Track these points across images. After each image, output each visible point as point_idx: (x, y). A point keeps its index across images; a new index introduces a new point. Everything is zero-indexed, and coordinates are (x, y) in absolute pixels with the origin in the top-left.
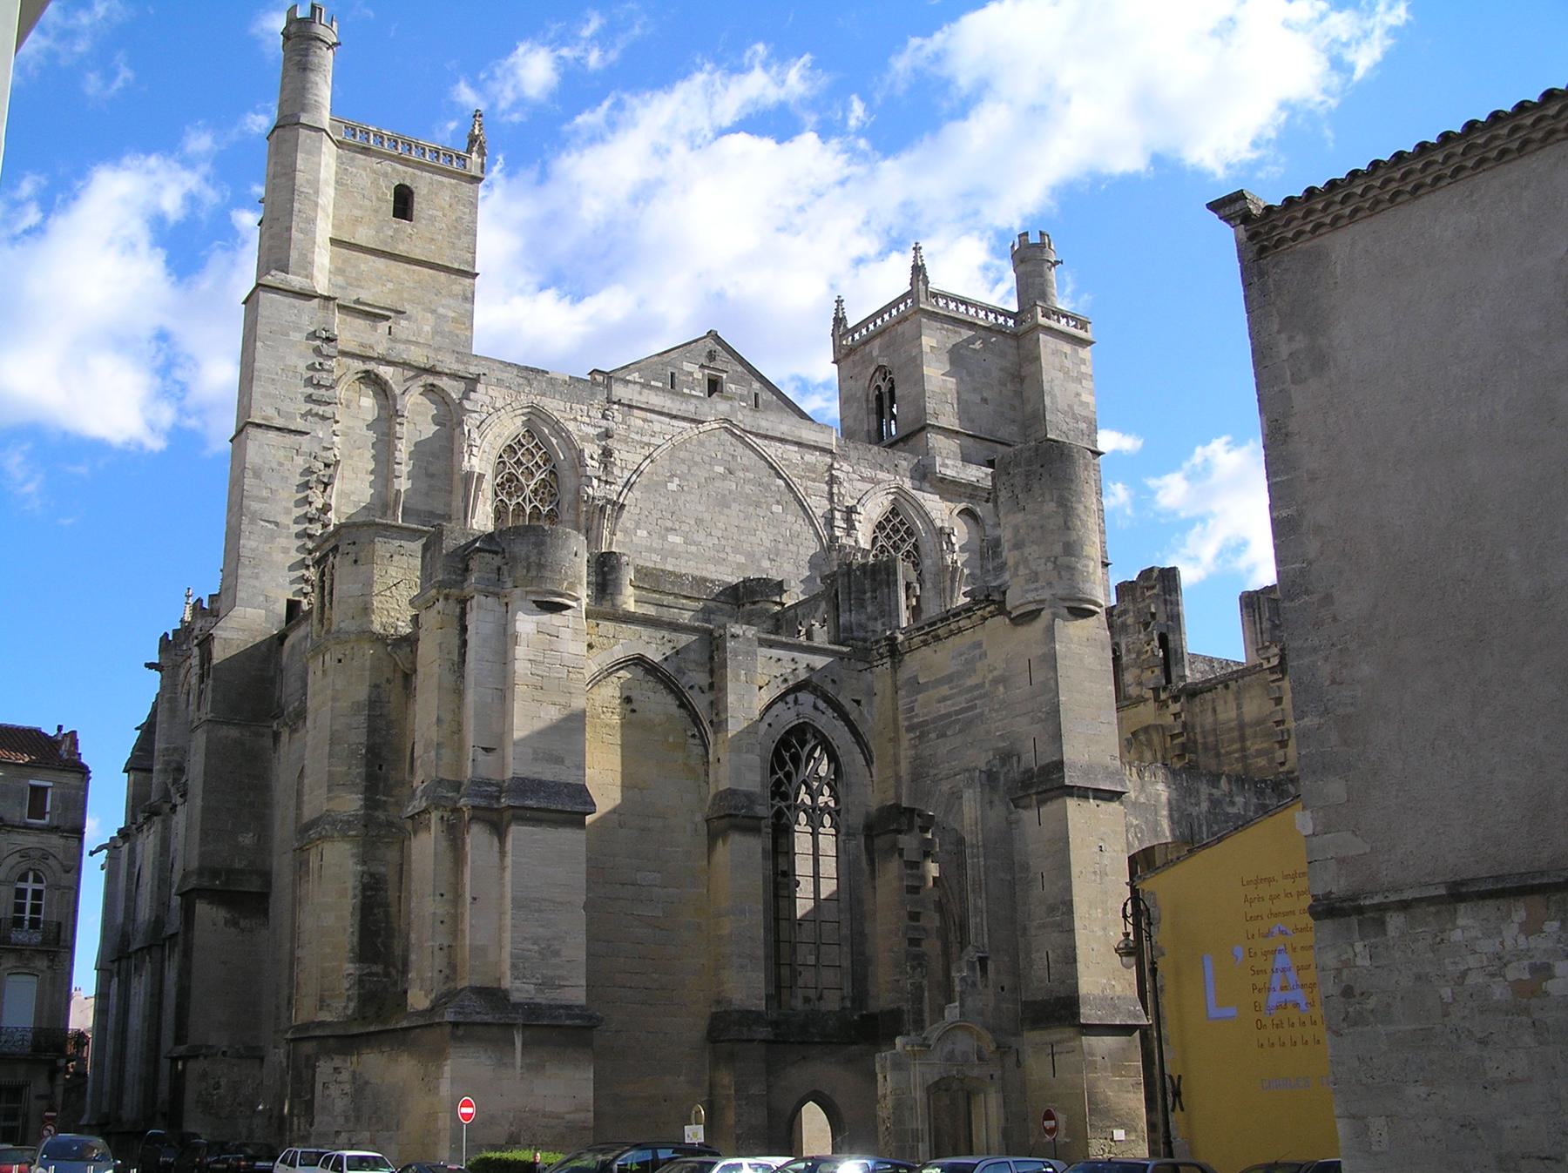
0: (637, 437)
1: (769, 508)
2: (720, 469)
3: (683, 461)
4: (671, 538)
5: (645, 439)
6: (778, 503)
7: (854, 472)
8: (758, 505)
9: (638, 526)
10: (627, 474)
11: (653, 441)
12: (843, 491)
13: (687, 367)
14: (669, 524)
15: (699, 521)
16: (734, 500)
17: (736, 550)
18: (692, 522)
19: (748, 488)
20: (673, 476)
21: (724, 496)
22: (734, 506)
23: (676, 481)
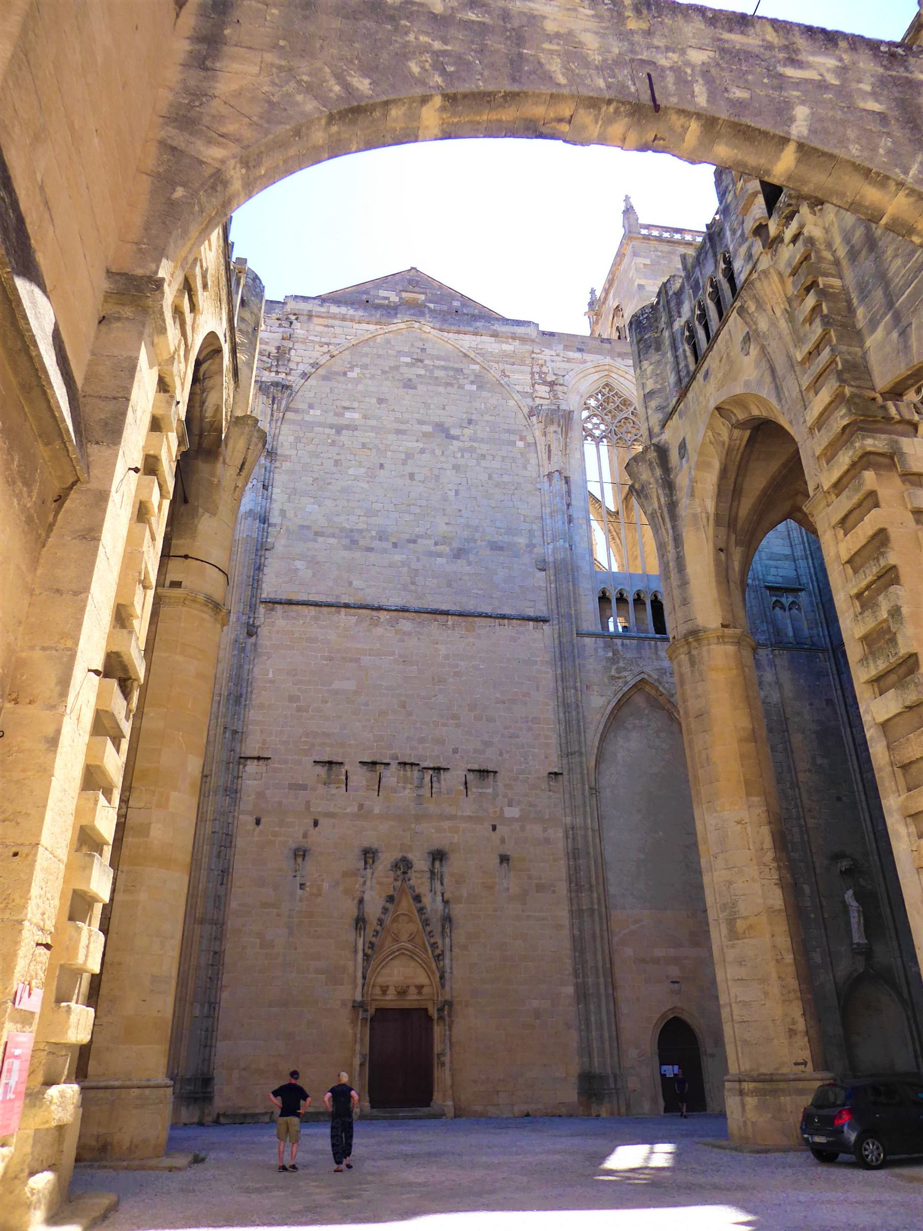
0: (317, 339)
1: (461, 387)
2: (408, 360)
3: (366, 355)
4: (348, 415)
5: (323, 340)
6: (472, 383)
7: (558, 355)
8: (448, 384)
9: (311, 406)
10: (302, 367)
11: (333, 340)
12: (544, 369)
13: (382, 293)
14: (346, 404)
15: (380, 401)
16: (422, 383)
17: (421, 422)
18: (374, 401)
19: (439, 373)
20: (352, 368)
21: (410, 380)
22: (419, 387)
23: (357, 370)
